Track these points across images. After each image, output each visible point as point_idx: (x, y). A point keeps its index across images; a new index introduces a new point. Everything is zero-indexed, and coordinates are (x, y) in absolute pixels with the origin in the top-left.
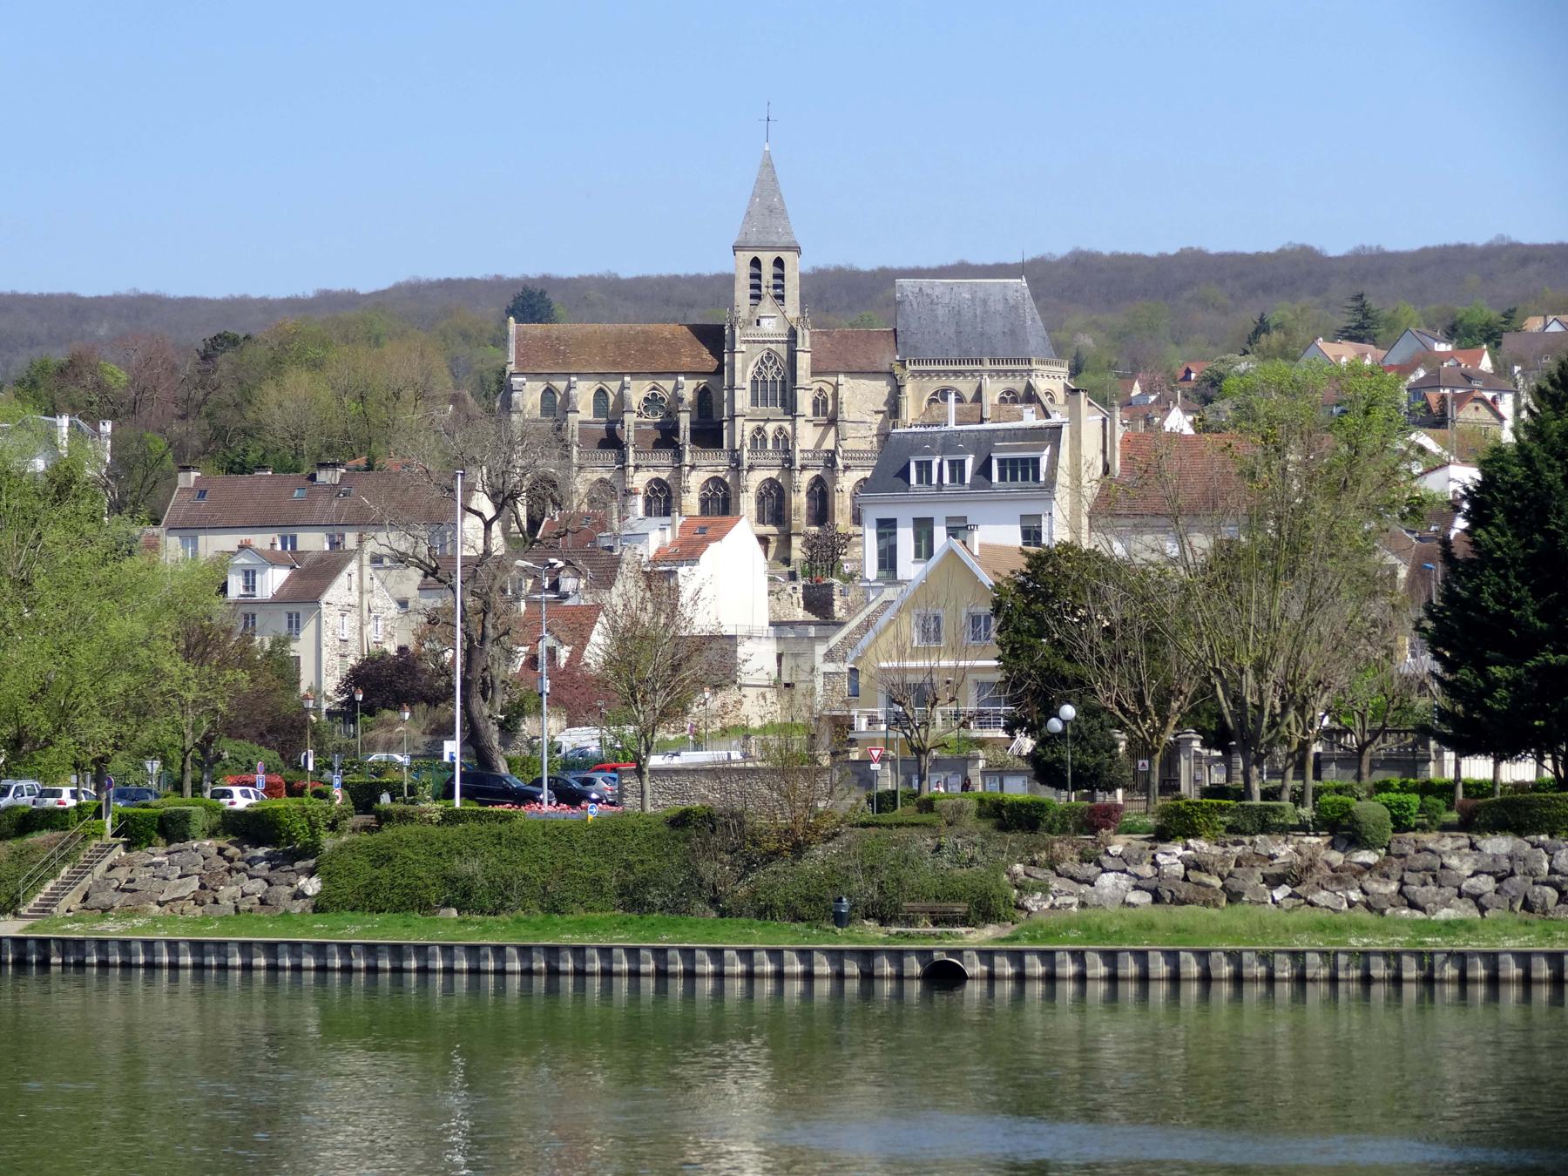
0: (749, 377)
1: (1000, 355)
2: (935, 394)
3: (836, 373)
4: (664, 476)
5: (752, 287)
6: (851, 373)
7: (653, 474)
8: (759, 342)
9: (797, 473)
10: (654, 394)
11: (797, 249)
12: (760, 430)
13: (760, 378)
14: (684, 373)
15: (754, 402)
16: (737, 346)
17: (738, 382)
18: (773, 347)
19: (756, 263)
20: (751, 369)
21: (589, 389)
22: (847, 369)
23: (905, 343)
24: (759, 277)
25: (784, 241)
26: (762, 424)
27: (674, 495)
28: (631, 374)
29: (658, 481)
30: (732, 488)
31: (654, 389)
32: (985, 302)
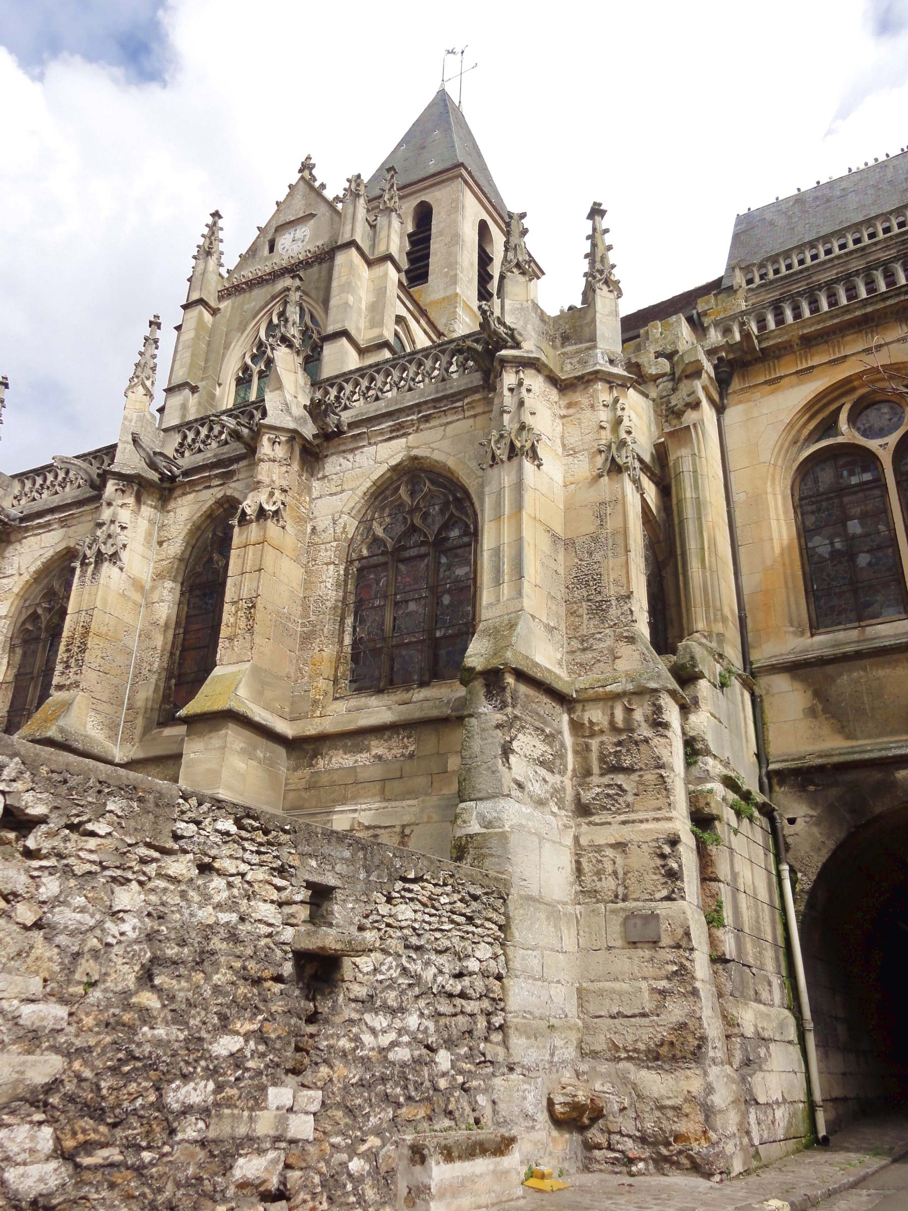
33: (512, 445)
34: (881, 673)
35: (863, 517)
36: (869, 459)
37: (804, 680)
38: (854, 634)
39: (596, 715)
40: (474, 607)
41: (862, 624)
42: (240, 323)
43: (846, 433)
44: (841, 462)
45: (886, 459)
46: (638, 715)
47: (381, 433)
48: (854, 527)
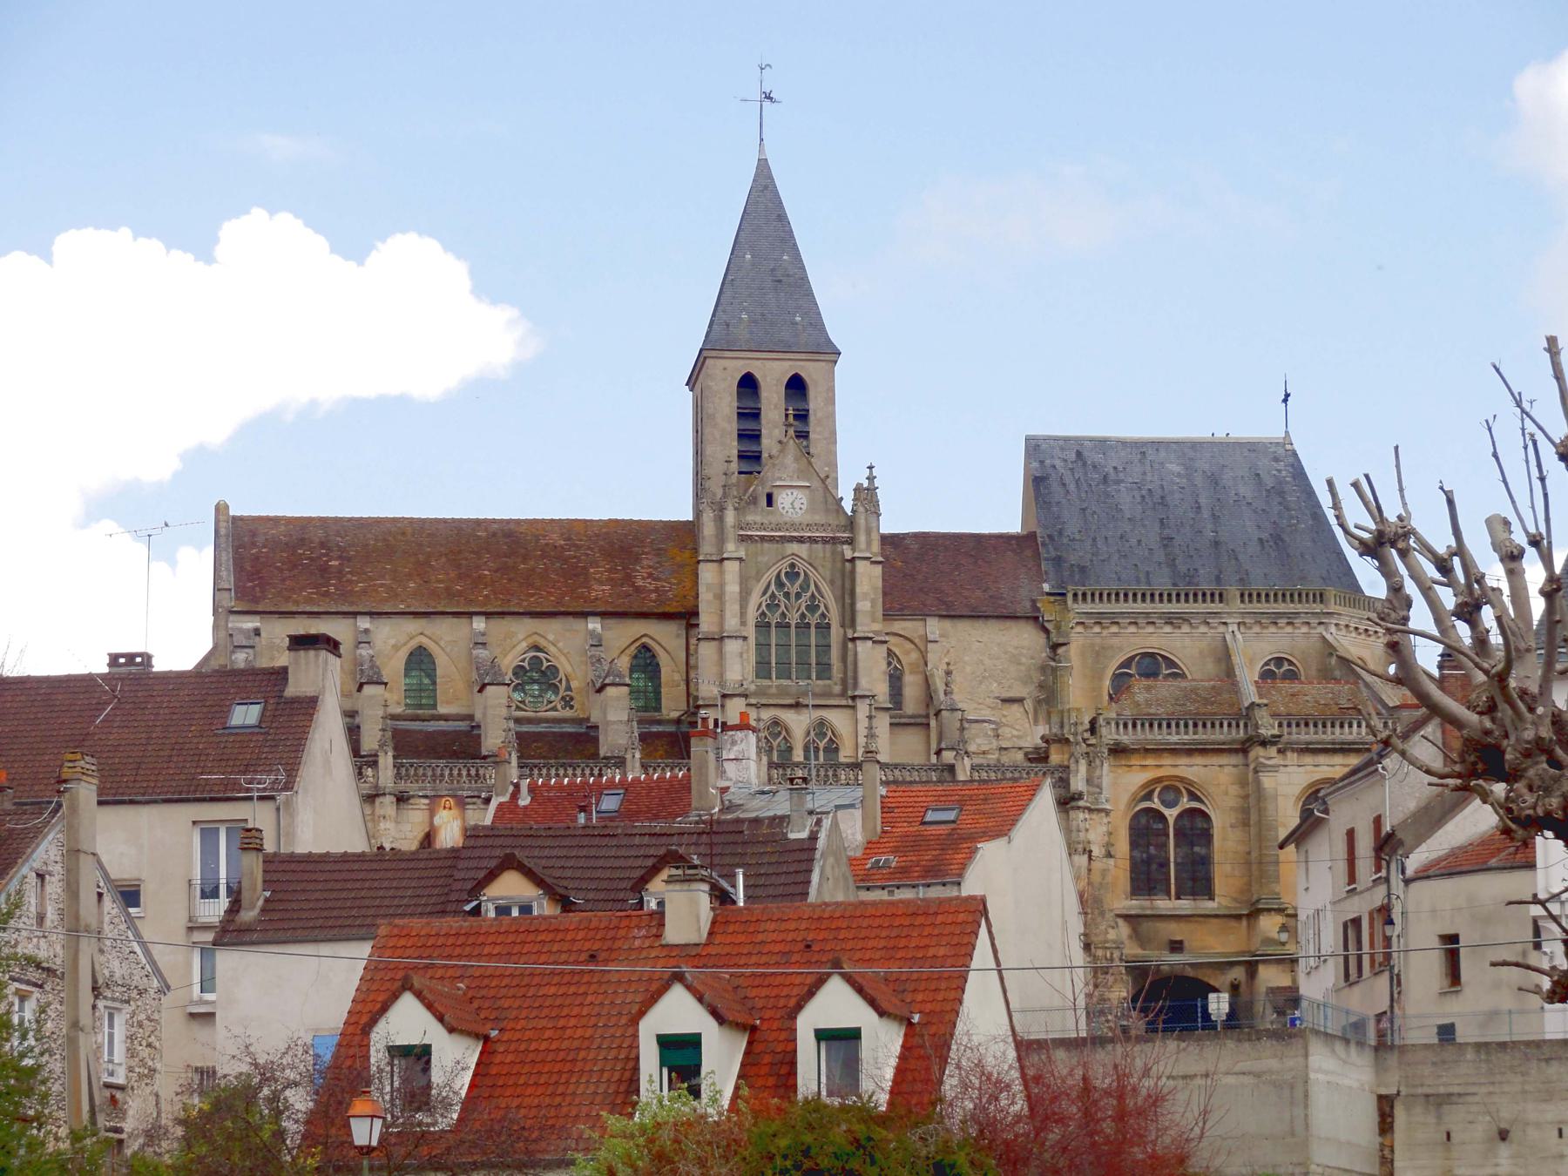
0: (752, 615)
1: (1257, 586)
2: (1127, 663)
5: (743, 436)
8: (772, 539)
13: (774, 619)
15: (763, 669)
17: (732, 623)
18: (802, 550)
19: (748, 384)
23: (1058, 561)
24: (755, 415)
32: (1214, 481)
34: (1158, 924)
35: (1157, 846)
36: (1162, 818)
37: (1129, 922)
38: (1147, 903)
39: (1100, 953)
41: (1153, 897)
42: (757, 573)
43: (1156, 804)
44: (1151, 815)
45: (1171, 822)
46: (1115, 956)
48: (1152, 850)
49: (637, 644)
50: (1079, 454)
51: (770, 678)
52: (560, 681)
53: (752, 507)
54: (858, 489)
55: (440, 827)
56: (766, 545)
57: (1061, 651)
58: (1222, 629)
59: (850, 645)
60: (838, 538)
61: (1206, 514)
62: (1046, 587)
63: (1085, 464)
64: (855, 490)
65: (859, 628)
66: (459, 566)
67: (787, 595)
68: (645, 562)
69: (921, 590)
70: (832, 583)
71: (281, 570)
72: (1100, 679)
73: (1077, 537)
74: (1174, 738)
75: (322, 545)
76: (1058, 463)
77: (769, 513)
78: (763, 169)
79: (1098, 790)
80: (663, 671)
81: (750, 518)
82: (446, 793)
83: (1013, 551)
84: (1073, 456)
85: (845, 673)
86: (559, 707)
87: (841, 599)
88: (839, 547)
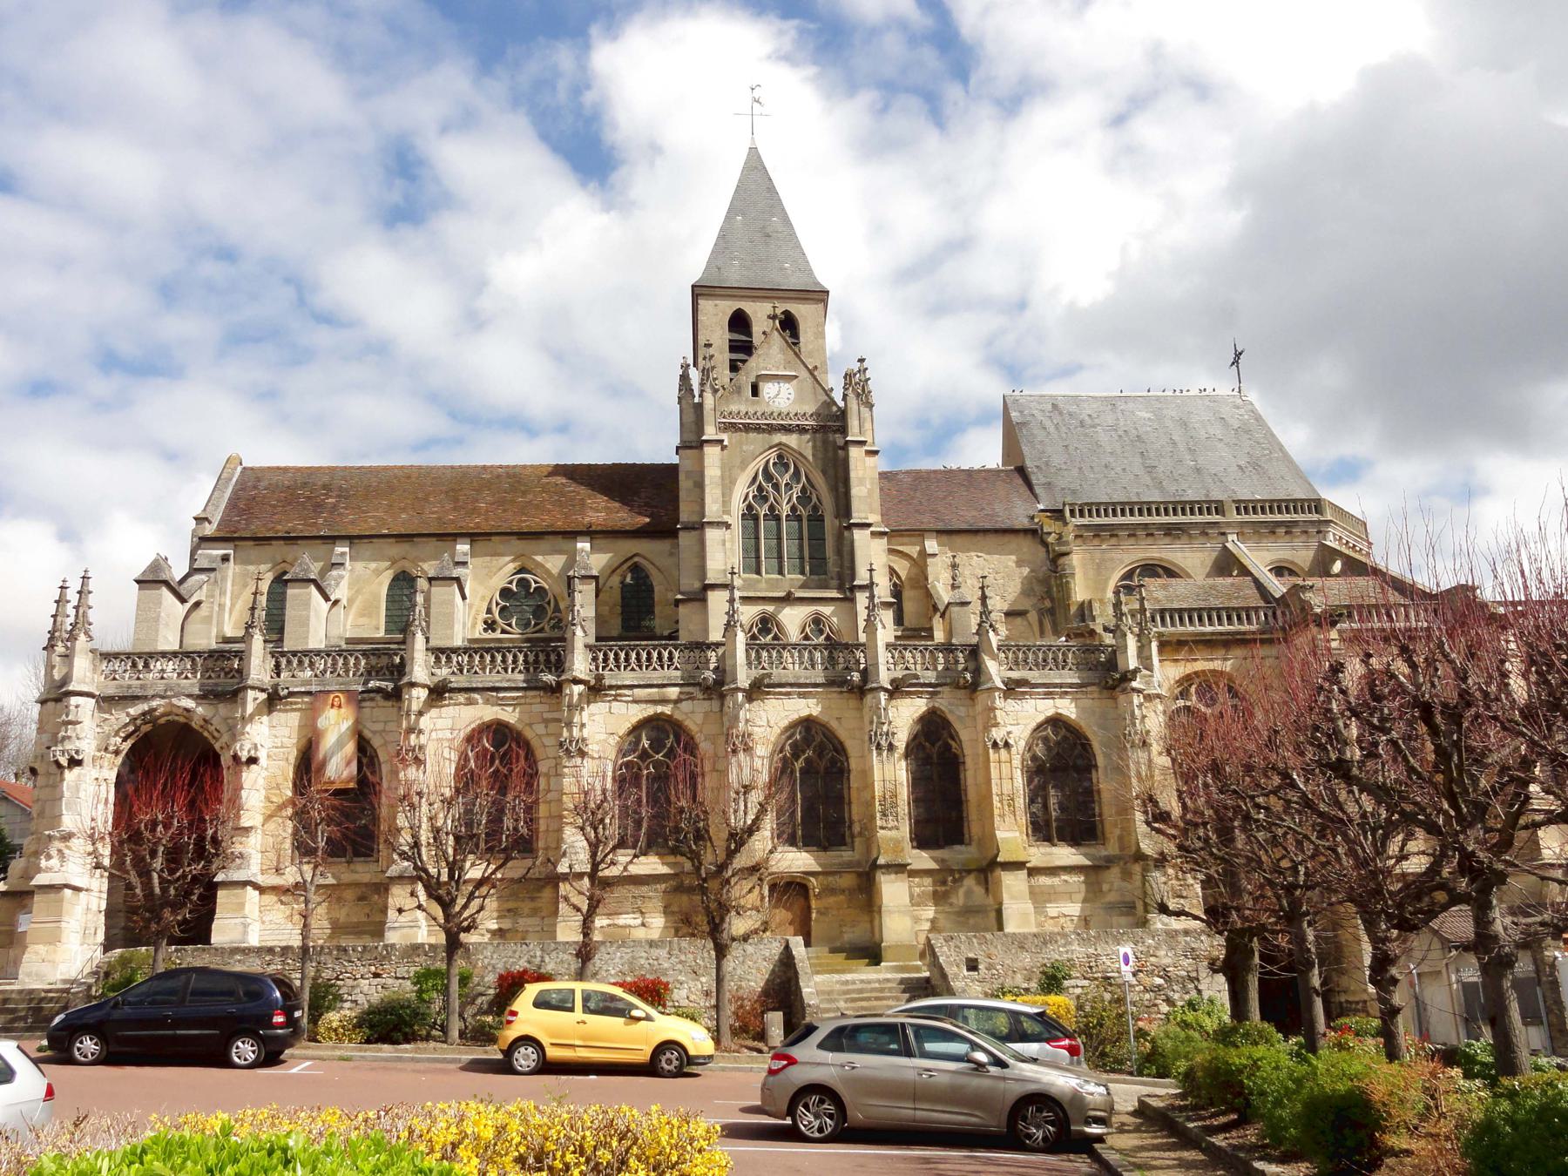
0: (737, 506)
3: (919, 533)
4: (510, 716)
6: (945, 533)
7: (485, 712)
9: (883, 696)
10: (523, 583)
11: (819, 296)
12: (766, 624)
13: (763, 510)
14: (590, 533)
15: (753, 564)
16: (710, 432)
17: (712, 510)
18: (792, 440)
20: (742, 488)
21: (378, 573)
22: (941, 526)
25: (795, 282)
26: (770, 608)
27: (543, 767)
28: (473, 537)
29: (499, 732)
30: (704, 746)
31: (521, 570)
32: (1184, 424)
33: (1144, 742)
40: (1100, 808)
47: (1039, 693)
49: (629, 564)
50: (1055, 406)
51: (758, 572)
52: (549, 603)
53: (736, 395)
54: (848, 376)
55: (327, 729)
56: (752, 435)
57: (1062, 561)
58: (1221, 538)
59: (846, 533)
60: (830, 427)
61: (1182, 447)
62: (1041, 507)
63: (1061, 413)
64: (845, 378)
65: (854, 515)
66: (456, 500)
67: (776, 487)
68: (643, 495)
69: (917, 511)
70: (824, 472)
71: (274, 507)
72: (1104, 590)
73: (1064, 467)
74: (1209, 629)
75: (325, 487)
76: (1035, 412)
77: (753, 403)
78: (754, 156)
79: (1148, 673)
80: (656, 589)
81: (734, 408)
82: (337, 687)
83: (1004, 481)
84: (1049, 407)
85: (841, 566)
86: (547, 628)
87: (834, 489)
88: (831, 436)
